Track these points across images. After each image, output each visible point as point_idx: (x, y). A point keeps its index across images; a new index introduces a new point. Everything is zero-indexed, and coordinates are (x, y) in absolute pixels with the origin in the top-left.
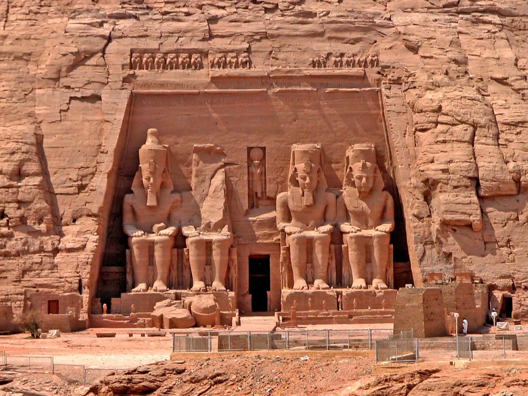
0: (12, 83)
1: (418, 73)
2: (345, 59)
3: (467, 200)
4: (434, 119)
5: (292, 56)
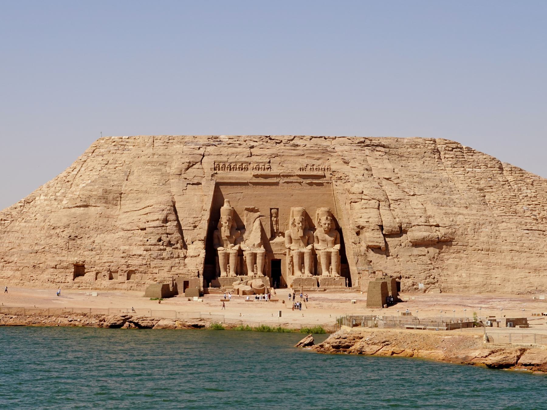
1: (350, 175)
2: (315, 167)
3: (378, 236)
4: (360, 197)
5: (290, 166)
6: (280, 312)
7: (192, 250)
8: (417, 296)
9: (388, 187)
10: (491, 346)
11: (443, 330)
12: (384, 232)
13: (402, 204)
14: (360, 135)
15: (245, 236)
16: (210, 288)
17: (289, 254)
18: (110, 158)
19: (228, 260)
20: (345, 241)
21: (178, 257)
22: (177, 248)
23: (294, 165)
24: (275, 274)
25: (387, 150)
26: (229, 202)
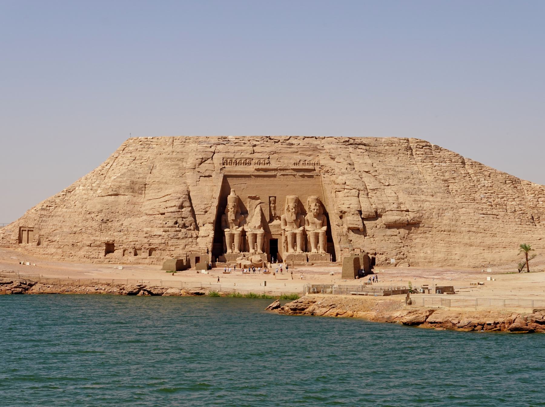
0: (177, 170)
1: (336, 168)
2: (306, 162)
3: (357, 219)
5: (286, 161)
6: (265, 282)
7: (203, 231)
8: (387, 269)
9: (366, 179)
10: (409, 308)
11: (381, 295)
12: (362, 216)
13: (378, 192)
14: (346, 135)
15: (248, 219)
16: (217, 262)
17: (284, 235)
18: (137, 155)
19: (233, 239)
20: (331, 224)
21: (192, 237)
22: (190, 230)
23: (289, 161)
24: (272, 250)
25: (368, 148)
26: (234, 191)
